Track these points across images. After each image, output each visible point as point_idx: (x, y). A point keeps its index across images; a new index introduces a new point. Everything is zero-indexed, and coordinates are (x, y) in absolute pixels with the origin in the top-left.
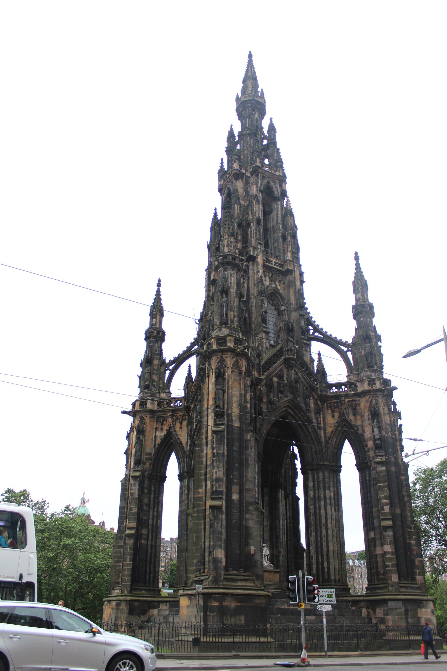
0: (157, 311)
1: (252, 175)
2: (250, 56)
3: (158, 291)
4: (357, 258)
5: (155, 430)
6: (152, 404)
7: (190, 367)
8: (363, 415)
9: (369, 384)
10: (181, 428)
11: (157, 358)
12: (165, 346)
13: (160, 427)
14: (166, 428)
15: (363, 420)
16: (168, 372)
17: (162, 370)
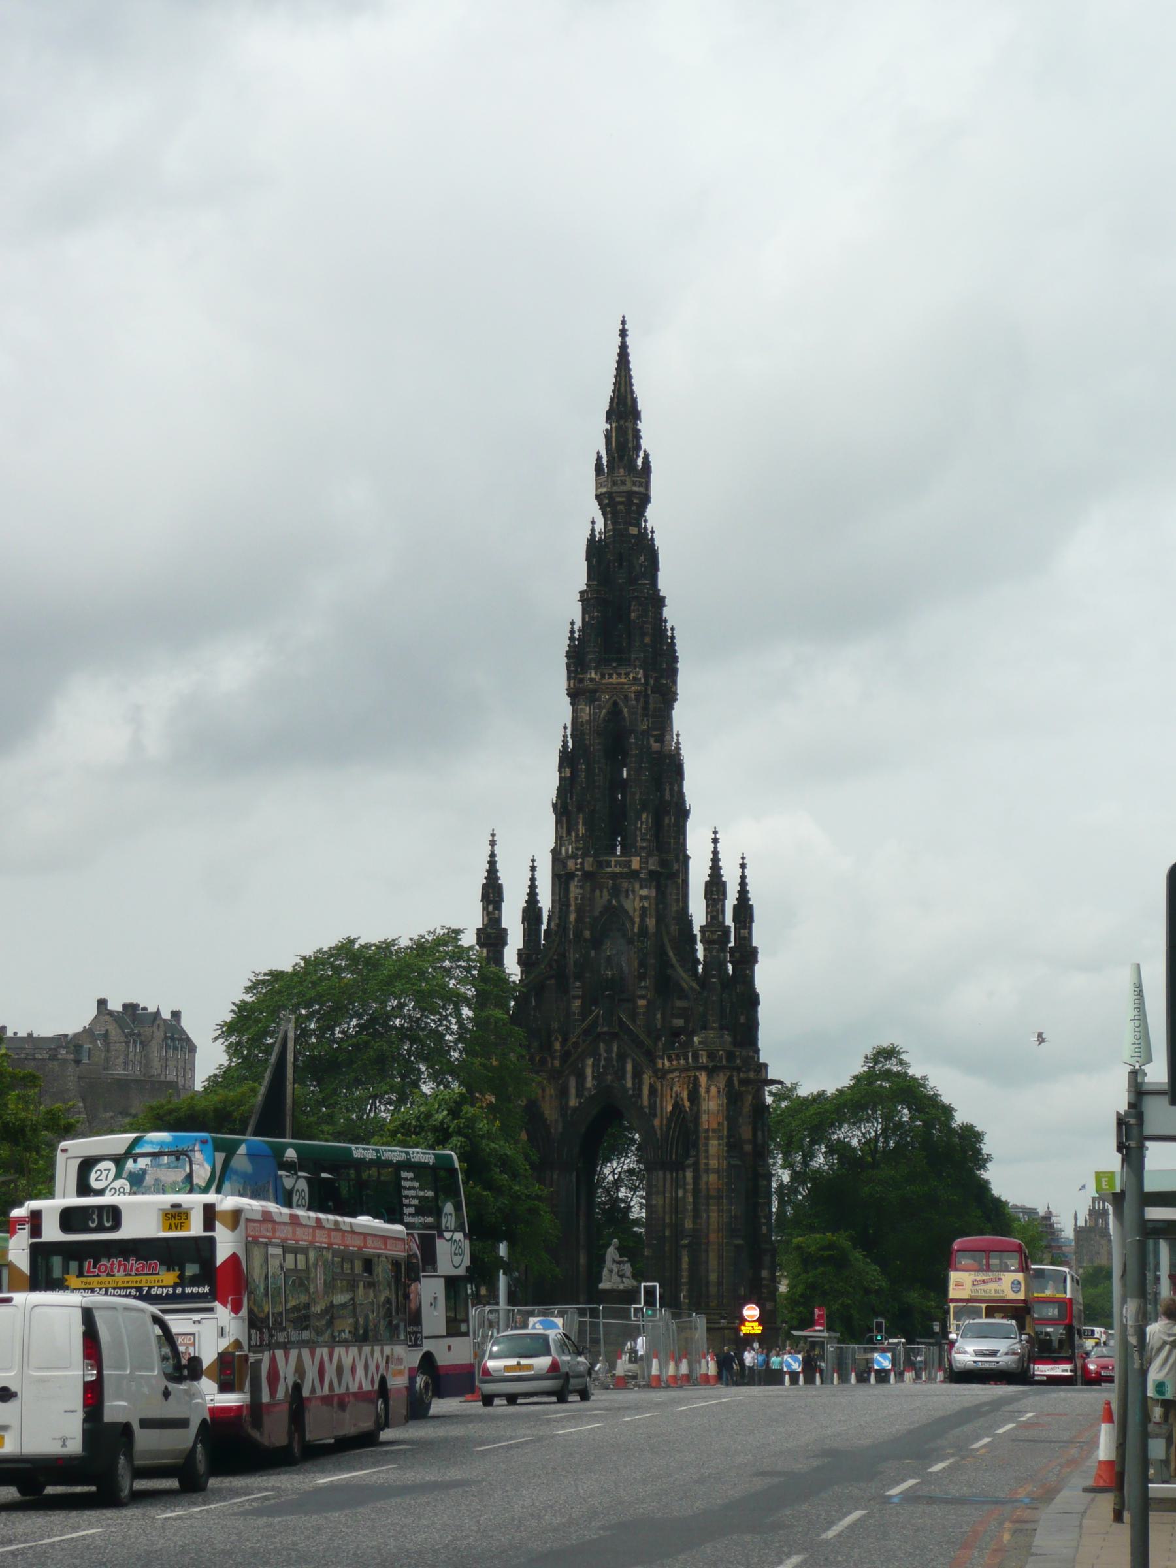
1: (652, 692)
2: (623, 333)
3: (493, 855)
10: (543, 1097)
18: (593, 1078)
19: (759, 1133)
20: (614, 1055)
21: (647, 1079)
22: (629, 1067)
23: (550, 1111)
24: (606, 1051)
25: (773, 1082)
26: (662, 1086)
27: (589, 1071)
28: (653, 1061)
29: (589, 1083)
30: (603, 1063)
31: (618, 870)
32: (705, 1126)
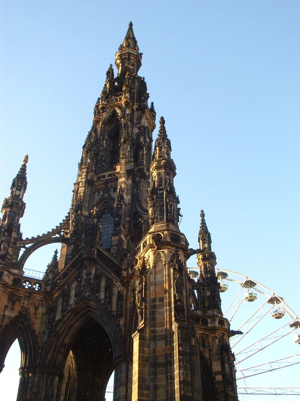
0: (20, 183)
2: (131, 25)
4: (203, 215)
5: (3, 308)
6: (9, 277)
7: (56, 252)
8: (212, 350)
9: (219, 323)
10: (35, 314)
11: (15, 230)
12: (22, 221)
13: (10, 306)
14: (17, 308)
15: (211, 353)
16: (23, 250)
17: (18, 245)
18: (76, 296)
19: (227, 365)
20: (92, 277)
21: (115, 291)
22: (103, 283)
23: (38, 326)
24: (86, 275)
25: (234, 333)
26: (127, 291)
27: (73, 293)
28: (119, 274)
29: (72, 301)
30: (83, 283)
31: (110, 177)
32: (152, 297)
